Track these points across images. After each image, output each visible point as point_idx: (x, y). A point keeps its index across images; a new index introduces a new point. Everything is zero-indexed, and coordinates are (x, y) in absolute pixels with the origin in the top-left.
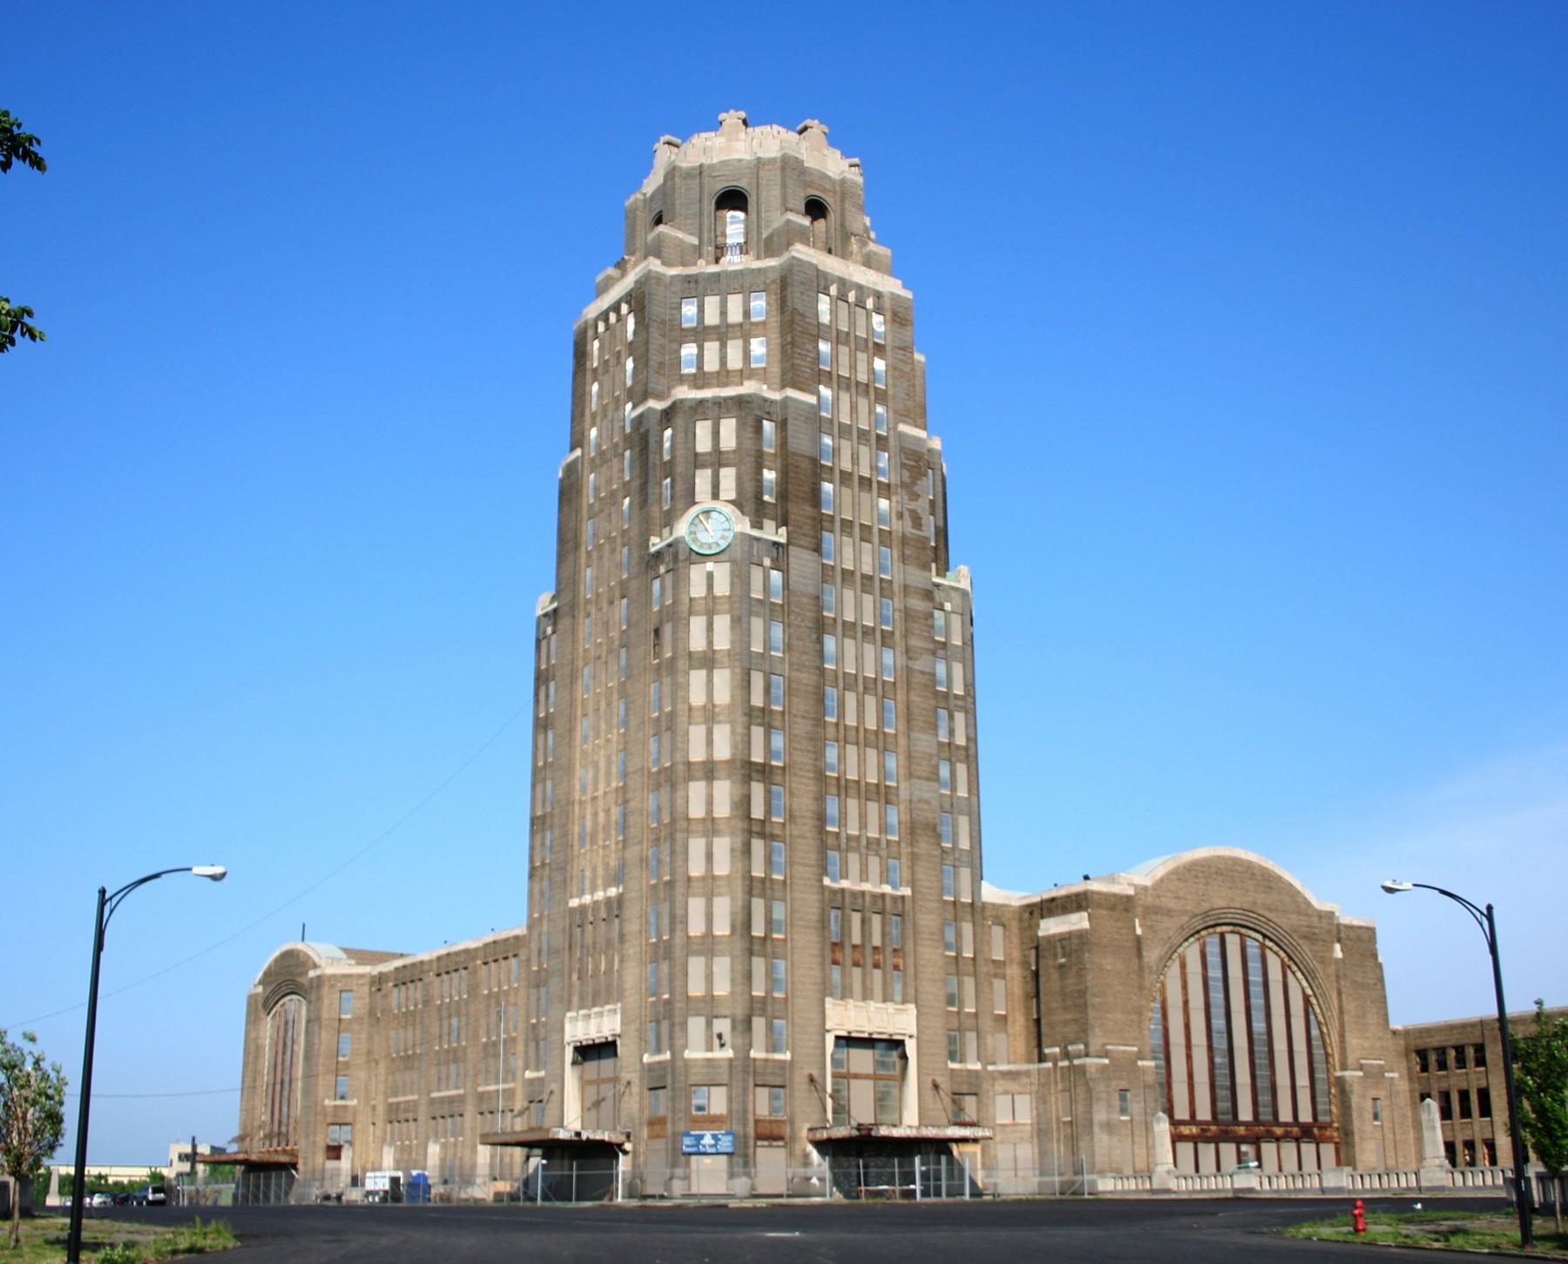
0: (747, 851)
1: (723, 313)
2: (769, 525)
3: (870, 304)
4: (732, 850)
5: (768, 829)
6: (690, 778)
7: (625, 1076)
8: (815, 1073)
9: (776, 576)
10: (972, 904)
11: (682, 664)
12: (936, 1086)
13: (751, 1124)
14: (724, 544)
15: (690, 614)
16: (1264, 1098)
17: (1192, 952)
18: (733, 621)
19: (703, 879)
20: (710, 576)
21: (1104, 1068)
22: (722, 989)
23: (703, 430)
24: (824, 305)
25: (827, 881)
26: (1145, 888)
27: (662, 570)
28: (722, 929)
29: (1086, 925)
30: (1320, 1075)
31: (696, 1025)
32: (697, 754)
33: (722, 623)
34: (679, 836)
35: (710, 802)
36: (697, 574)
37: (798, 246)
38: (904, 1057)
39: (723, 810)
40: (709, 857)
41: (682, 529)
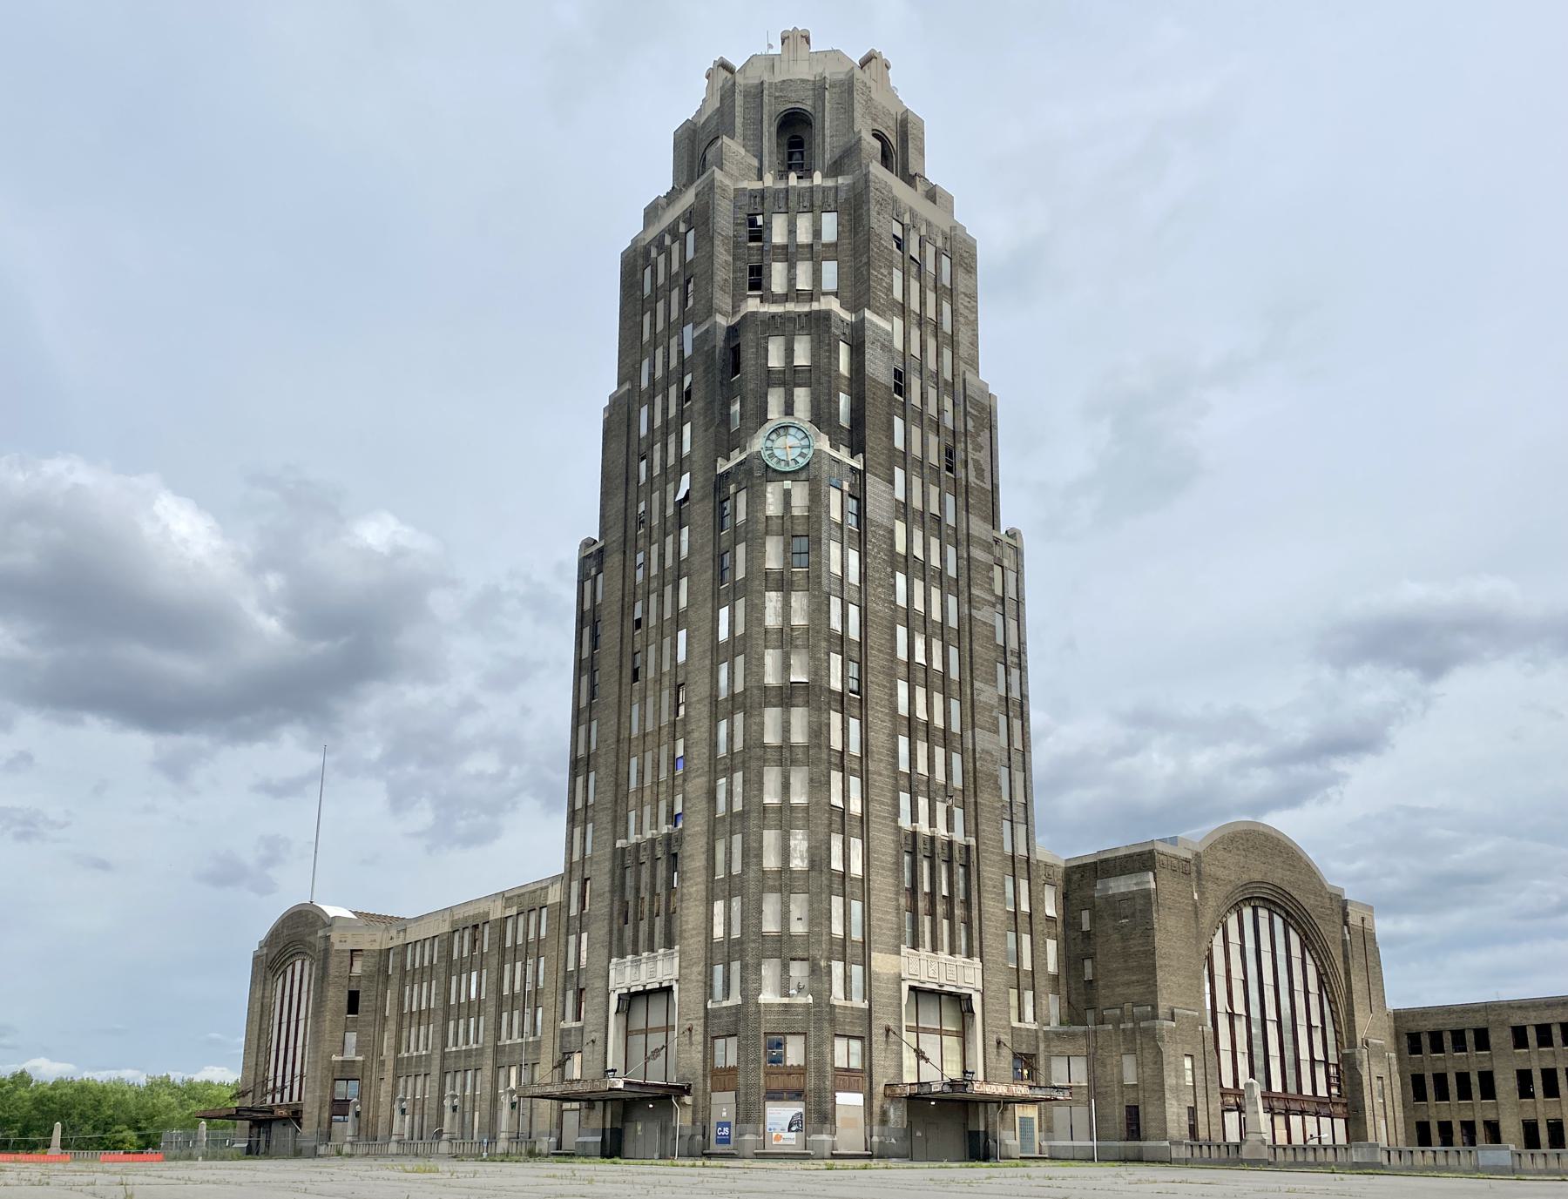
4: (811, 780)
8: (892, 1025)
11: (757, 584)
15: (767, 533)
16: (1291, 1073)
17: (1232, 922)
19: (780, 809)
20: (787, 494)
21: (1171, 1031)
27: (732, 488)
28: (798, 863)
32: (771, 679)
34: (754, 764)
35: (786, 729)
39: (798, 737)
40: (786, 787)
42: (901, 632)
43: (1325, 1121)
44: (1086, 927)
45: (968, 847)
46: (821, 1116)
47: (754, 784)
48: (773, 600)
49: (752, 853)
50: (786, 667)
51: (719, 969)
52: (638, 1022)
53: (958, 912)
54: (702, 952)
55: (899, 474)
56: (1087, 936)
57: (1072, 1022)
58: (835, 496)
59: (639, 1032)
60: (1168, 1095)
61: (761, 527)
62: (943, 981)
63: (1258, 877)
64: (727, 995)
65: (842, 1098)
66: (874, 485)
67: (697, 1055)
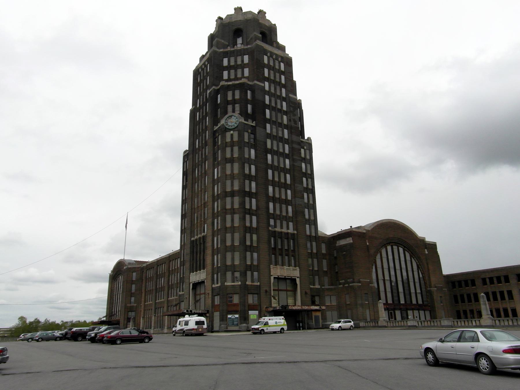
0: (244, 219)
1: (236, 61)
2: (250, 121)
3: (280, 59)
5: (251, 212)
6: (226, 196)
7: (207, 292)
8: (268, 289)
9: (252, 136)
10: (315, 236)
12: (306, 293)
13: (247, 306)
14: (236, 125)
16: (408, 297)
18: (239, 148)
19: (231, 227)
20: (232, 135)
21: (359, 287)
22: (237, 262)
23: (230, 94)
24: (266, 58)
25: (270, 228)
26: (368, 231)
28: (237, 243)
29: (352, 241)
30: (423, 289)
31: (229, 275)
33: (236, 149)
35: (232, 203)
36: (228, 135)
37: (258, 41)
38: (296, 284)
39: (236, 206)
41: (223, 122)
42: (270, 172)
43: (422, 312)
44: (335, 255)
45: (294, 234)
46: (245, 318)
47: (224, 220)
48: (228, 166)
49: (224, 241)
50: (232, 185)
51: (215, 275)
52: (198, 292)
53: (291, 253)
54: (211, 271)
55: (268, 126)
56: (336, 258)
57: (332, 285)
58: (246, 135)
59: (198, 295)
60: (358, 306)
61: (224, 145)
62: (285, 275)
63: (392, 236)
64: (217, 283)
65: (250, 312)
66: (259, 130)
67: (209, 301)
